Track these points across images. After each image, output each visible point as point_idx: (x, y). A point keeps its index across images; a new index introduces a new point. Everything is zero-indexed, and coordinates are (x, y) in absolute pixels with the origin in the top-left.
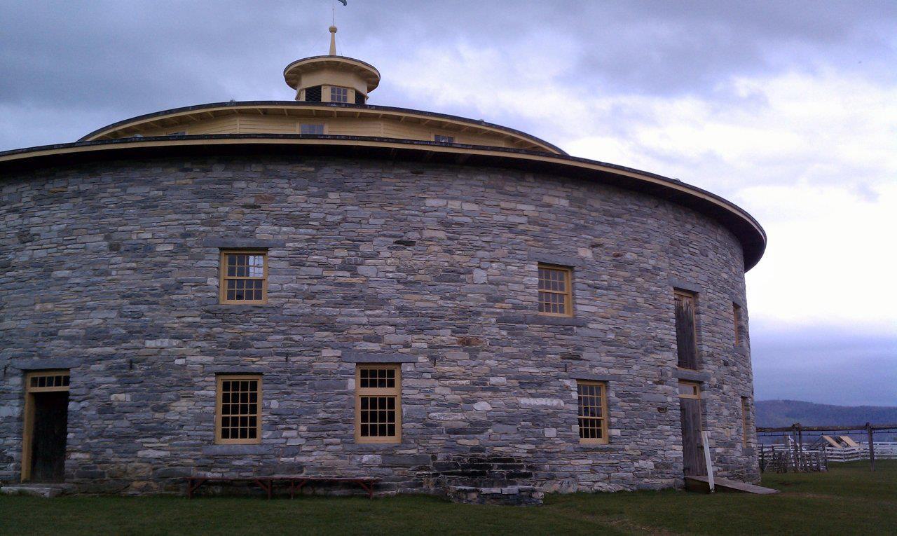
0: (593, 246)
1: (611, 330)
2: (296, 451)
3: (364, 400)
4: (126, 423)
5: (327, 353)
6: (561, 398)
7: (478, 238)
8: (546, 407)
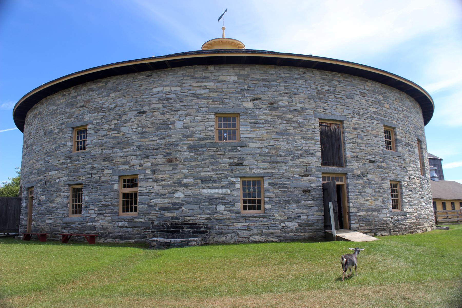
0: (253, 100)
1: (267, 148)
2: (93, 220)
3: (124, 194)
4: (43, 209)
5: (106, 172)
6: (228, 188)
7: (179, 104)
8: (218, 194)
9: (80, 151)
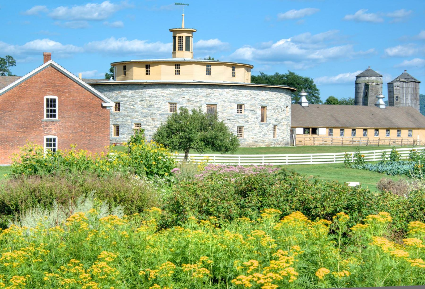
5: (129, 121)
9: (116, 111)
